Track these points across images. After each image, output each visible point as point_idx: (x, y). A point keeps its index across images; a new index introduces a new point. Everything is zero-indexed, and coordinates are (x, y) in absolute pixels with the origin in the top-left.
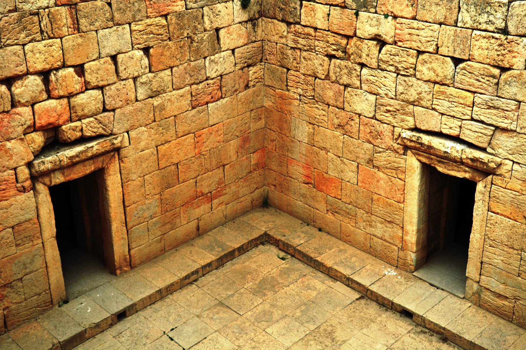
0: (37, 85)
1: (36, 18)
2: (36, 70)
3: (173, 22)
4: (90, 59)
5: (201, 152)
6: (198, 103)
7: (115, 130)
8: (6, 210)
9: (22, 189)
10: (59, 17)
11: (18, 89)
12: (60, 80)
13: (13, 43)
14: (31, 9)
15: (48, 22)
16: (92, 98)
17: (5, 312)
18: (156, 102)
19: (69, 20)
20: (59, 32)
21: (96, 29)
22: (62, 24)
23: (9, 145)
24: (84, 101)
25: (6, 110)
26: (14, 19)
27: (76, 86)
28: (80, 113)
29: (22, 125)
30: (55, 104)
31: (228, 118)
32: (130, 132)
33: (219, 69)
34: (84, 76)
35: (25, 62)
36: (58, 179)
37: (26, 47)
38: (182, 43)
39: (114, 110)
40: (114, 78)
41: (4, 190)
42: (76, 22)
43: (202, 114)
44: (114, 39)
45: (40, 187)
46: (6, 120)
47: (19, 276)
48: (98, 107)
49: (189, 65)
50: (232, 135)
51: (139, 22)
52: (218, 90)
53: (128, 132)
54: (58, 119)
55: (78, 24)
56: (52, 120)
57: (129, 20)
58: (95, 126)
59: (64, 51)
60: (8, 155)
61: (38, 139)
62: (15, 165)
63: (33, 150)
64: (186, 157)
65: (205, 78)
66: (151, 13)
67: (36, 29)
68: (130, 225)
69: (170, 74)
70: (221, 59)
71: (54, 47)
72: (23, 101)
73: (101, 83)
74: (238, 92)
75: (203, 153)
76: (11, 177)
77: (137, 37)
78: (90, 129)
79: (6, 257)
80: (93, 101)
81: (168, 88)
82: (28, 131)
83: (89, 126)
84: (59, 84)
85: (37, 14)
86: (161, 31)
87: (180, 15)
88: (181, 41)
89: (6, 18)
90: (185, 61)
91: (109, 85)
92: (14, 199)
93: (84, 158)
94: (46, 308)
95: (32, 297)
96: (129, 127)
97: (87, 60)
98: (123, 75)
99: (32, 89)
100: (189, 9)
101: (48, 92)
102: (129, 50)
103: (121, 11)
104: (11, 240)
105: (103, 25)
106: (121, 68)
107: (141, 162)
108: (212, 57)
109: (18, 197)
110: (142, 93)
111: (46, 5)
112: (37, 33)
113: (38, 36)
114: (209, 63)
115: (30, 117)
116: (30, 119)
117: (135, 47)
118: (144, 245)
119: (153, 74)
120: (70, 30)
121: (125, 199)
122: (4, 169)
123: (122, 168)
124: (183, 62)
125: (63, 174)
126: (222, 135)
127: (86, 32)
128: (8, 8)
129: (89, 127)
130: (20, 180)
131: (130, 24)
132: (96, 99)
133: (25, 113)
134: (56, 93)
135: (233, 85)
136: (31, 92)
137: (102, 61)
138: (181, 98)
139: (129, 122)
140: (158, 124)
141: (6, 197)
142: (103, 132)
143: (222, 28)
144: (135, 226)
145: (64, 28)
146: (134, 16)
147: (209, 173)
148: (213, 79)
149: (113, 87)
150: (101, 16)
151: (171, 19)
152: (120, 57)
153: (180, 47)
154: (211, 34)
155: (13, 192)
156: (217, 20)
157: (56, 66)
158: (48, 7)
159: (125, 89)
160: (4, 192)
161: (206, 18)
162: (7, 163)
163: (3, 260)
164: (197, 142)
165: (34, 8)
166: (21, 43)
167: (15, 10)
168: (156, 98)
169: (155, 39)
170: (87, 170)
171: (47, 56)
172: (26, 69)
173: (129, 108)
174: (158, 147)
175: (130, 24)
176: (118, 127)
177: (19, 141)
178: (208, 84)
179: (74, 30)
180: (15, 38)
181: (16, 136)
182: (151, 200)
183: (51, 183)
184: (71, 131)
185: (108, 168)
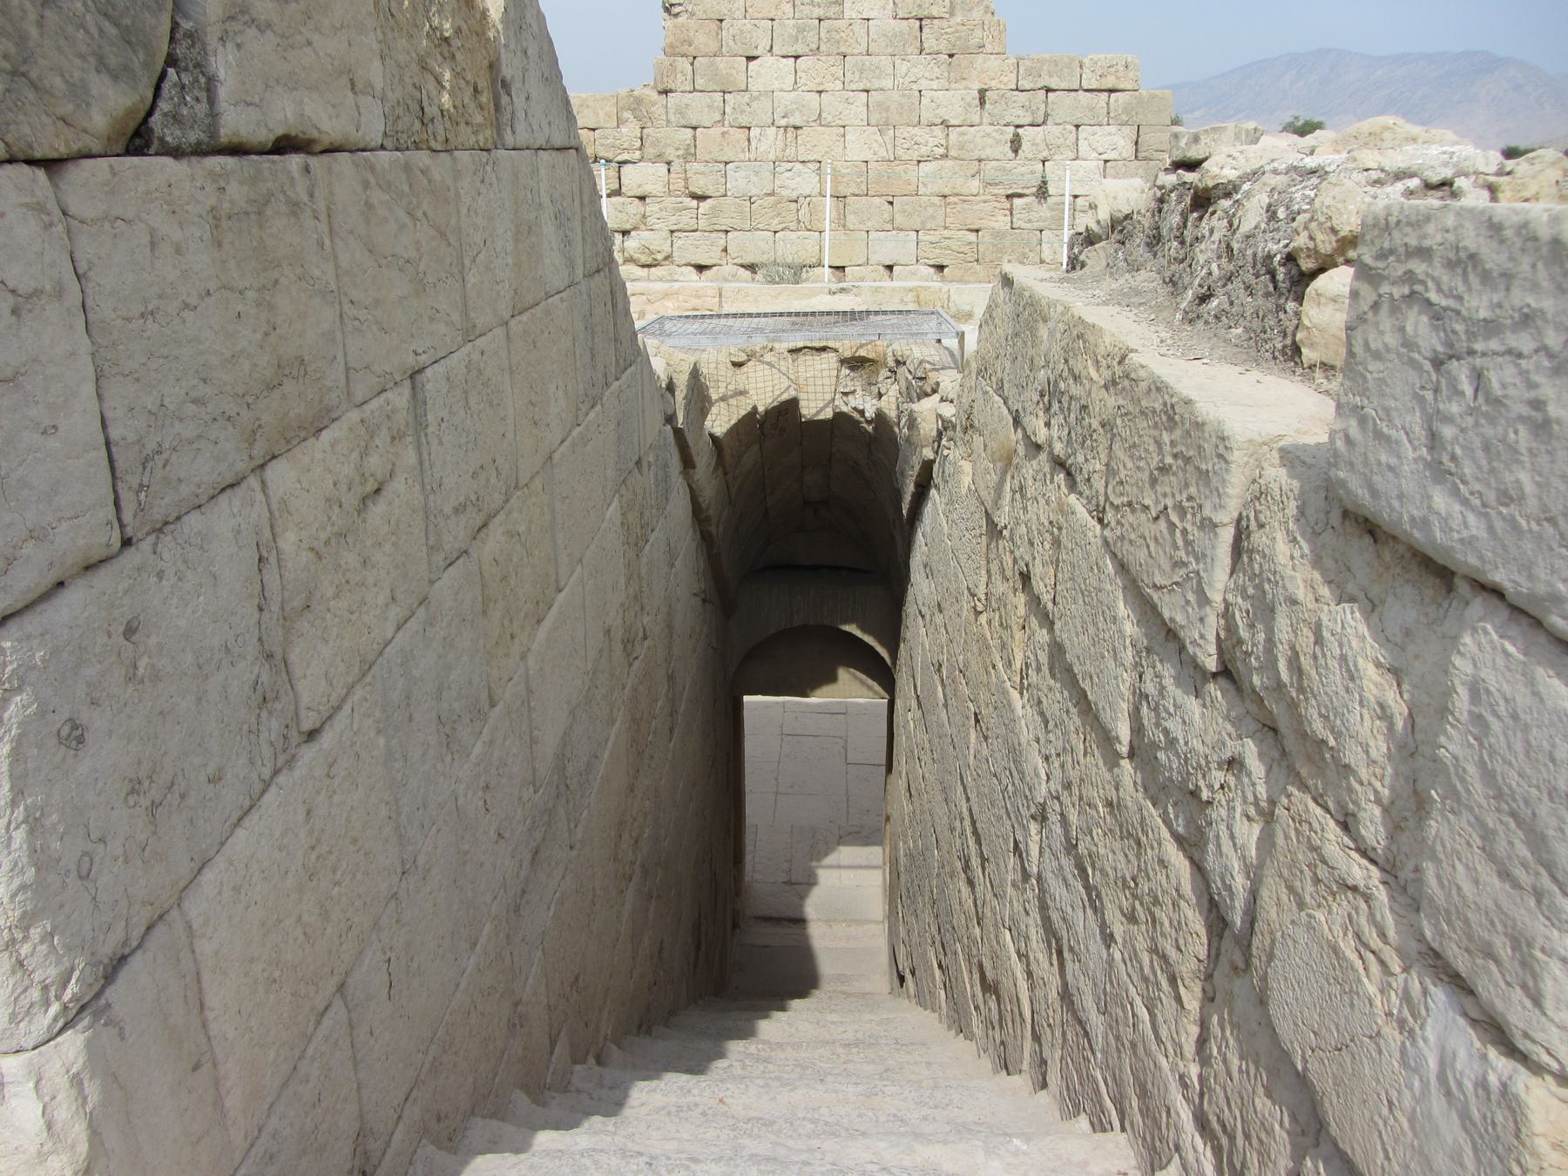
67: (793, 217)
86: (966, 249)
87: (997, 234)
105: (878, 226)
113: (793, 226)
146: (923, 223)
157: (808, 262)
165: (794, 195)
167: (772, 194)
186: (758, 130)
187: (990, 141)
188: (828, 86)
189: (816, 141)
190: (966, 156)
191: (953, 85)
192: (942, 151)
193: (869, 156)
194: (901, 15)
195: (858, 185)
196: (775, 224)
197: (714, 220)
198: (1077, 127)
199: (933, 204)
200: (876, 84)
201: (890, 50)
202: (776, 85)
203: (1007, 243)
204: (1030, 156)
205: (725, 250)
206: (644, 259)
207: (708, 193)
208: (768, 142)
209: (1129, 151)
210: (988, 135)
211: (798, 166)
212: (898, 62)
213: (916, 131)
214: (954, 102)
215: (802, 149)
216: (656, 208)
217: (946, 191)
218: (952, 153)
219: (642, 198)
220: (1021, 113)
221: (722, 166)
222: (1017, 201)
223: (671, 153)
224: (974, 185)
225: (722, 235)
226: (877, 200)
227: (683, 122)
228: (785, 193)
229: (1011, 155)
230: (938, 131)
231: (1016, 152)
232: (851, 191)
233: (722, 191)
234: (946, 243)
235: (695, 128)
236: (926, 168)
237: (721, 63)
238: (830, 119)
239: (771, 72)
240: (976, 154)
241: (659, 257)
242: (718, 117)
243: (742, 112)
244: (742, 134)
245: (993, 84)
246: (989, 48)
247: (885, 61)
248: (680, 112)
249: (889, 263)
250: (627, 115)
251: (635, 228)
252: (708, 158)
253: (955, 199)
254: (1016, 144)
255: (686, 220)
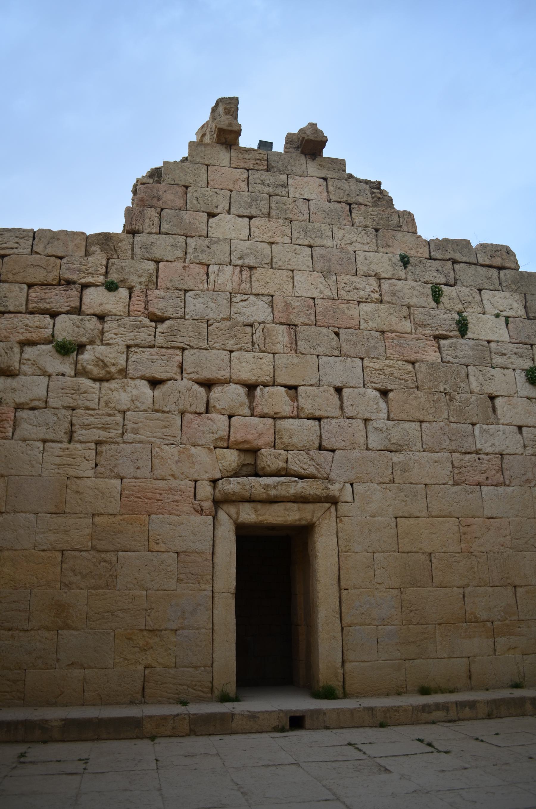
0: (238, 395)
1: (248, 329)
2: (239, 378)
3: (422, 370)
4: (306, 383)
5: (472, 550)
6: (463, 479)
7: (333, 475)
8: (175, 528)
9: (199, 509)
10: (275, 333)
11: (216, 392)
12: (266, 396)
13: (220, 348)
14: (246, 321)
15: (262, 335)
16: (305, 427)
17: (147, 672)
18: (396, 458)
19: (286, 339)
20: (273, 347)
21: (318, 354)
22: (277, 340)
23: (193, 450)
24: (293, 427)
25: (198, 411)
26: (226, 326)
27: (285, 407)
28: (286, 440)
29: (213, 433)
30: (257, 422)
31: (517, 516)
32: (354, 485)
33: (497, 444)
34: (298, 402)
35: (229, 368)
36: (248, 515)
37: (233, 354)
38: (436, 396)
39: (333, 451)
40: (338, 413)
41: (177, 501)
42: (294, 342)
43: (471, 495)
44: (338, 371)
45: (222, 515)
46: (195, 422)
47: (174, 627)
48: (312, 440)
49: (449, 426)
50: (526, 543)
51: (375, 360)
52: (497, 472)
53: (352, 485)
54: (257, 439)
55: (296, 346)
56: (249, 437)
57: (360, 354)
58: (305, 461)
59: (276, 367)
60: (190, 461)
61: (231, 458)
62: (195, 477)
63: (221, 468)
64: (444, 549)
65: (474, 449)
66: (392, 354)
68: (347, 620)
69: (419, 429)
70: (501, 433)
71: (264, 361)
72: (218, 407)
73: (318, 413)
74: (532, 485)
75: (475, 553)
76: (189, 489)
77: (371, 375)
78: (298, 462)
79: (162, 590)
80: (305, 431)
81: (415, 445)
82: (219, 444)
83: (298, 462)
84: (264, 400)
85: (251, 326)
87: (431, 365)
88: (434, 394)
89: (218, 324)
90: (441, 419)
91: (328, 418)
92: (187, 517)
93: (283, 493)
94: (202, 694)
95: (185, 666)
96: (353, 477)
97: (303, 383)
98: (349, 411)
99: (231, 397)
100: (445, 362)
101: (252, 409)
102: (359, 386)
103: (351, 343)
104: (172, 569)
105: (328, 352)
106: (346, 403)
107: (370, 530)
108: (485, 426)
109: (192, 517)
110: (375, 441)
111: (262, 320)
112: (247, 343)
113: (249, 346)
114: (480, 432)
115: (224, 428)
116: (224, 430)
117: (368, 385)
118: (369, 664)
119: (392, 423)
120: (285, 348)
121: (341, 577)
122: (182, 476)
123: (339, 530)
124: (439, 420)
125: (256, 511)
126: (508, 538)
127: (303, 354)
128: (221, 315)
129: (296, 459)
130: (198, 497)
131: (362, 359)
132: (310, 429)
133: (219, 421)
134: (258, 410)
135: (523, 472)
136: (230, 400)
137: (322, 389)
138: (436, 464)
139: (354, 470)
140: (398, 487)
141: (178, 511)
142: (315, 472)
143: (498, 396)
144: (356, 624)
145: (278, 345)
146: (367, 352)
147: (487, 588)
148: (487, 454)
149: (334, 421)
150: (325, 342)
151: (420, 367)
152: (346, 392)
153: (434, 401)
154: (481, 398)
155: (187, 507)
156: (490, 384)
158: (264, 323)
159: (350, 429)
160: (177, 504)
161: (472, 378)
162: (187, 471)
163: (157, 592)
164: (464, 534)
165: (250, 321)
166: (228, 349)
167: (230, 319)
168: (397, 454)
169: (396, 383)
170: (289, 515)
171: (254, 367)
172: (228, 374)
173: (356, 454)
174: (398, 519)
175: (362, 359)
176: (338, 472)
177: (206, 450)
178: (479, 459)
179: (291, 350)
180: (222, 343)
181: (204, 443)
182: (385, 594)
183: (238, 517)
184: (272, 457)
185: (320, 524)
186: (216, 267)
187: (415, 293)
188: (278, 239)
189: (266, 280)
190: (398, 301)
191: (381, 249)
192: (377, 296)
193: (316, 294)
194: (333, 198)
195: (308, 316)
196: (231, 344)
197: (172, 338)
198: (480, 290)
199: (374, 337)
200: (319, 242)
201: (328, 220)
202: (233, 235)
203: (442, 374)
204: (449, 307)
205: (181, 367)
206: (96, 371)
207: (168, 314)
208: (226, 278)
209: (522, 312)
210: (413, 288)
211: (252, 298)
212: (335, 229)
213: (354, 278)
214: (383, 262)
215: (255, 285)
216: (114, 325)
217: (385, 328)
218: (386, 298)
219: (101, 318)
220: (436, 274)
221: (182, 293)
222: (442, 342)
223: (133, 280)
224: (407, 325)
225: (179, 352)
226: (324, 330)
227: (147, 255)
228: (241, 318)
229: (433, 304)
230: (373, 281)
231: (437, 301)
232: (301, 320)
233: (181, 313)
234: (388, 370)
235: (157, 262)
236: (366, 308)
237: (186, 216)
238: (280, 263)
239: (228, 226)
240: (406, 301)
241: (113, 369)
242: (180, 254)
243: (202, 251)
244: (202, 270)
245: (412, 253)
246: (405, 228)
247: (325, 228)
248: (144, 247)
249: (338, 385)
250: (95, 248)
251: (92, 342)
252: (169, 285)
253: (393, 335)
254: (437, 295)
255: (144, 336)
